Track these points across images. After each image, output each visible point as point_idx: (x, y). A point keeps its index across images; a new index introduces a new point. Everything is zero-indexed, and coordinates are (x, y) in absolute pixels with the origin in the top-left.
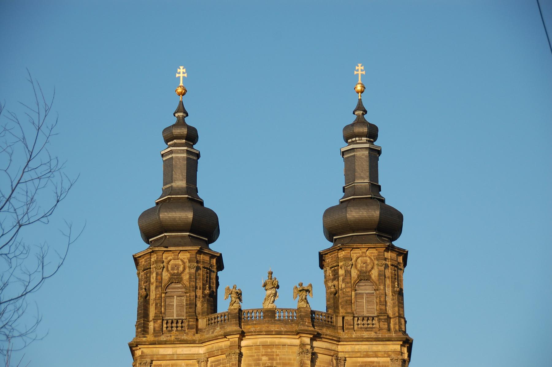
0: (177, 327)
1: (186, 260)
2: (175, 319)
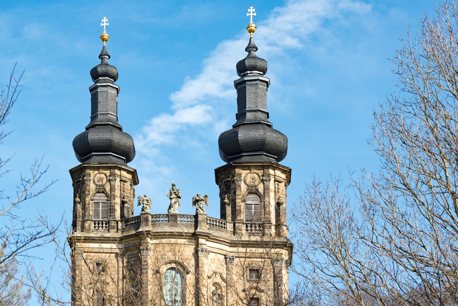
0: (102, 227)
1: (108, 174)
2: (101, 221)
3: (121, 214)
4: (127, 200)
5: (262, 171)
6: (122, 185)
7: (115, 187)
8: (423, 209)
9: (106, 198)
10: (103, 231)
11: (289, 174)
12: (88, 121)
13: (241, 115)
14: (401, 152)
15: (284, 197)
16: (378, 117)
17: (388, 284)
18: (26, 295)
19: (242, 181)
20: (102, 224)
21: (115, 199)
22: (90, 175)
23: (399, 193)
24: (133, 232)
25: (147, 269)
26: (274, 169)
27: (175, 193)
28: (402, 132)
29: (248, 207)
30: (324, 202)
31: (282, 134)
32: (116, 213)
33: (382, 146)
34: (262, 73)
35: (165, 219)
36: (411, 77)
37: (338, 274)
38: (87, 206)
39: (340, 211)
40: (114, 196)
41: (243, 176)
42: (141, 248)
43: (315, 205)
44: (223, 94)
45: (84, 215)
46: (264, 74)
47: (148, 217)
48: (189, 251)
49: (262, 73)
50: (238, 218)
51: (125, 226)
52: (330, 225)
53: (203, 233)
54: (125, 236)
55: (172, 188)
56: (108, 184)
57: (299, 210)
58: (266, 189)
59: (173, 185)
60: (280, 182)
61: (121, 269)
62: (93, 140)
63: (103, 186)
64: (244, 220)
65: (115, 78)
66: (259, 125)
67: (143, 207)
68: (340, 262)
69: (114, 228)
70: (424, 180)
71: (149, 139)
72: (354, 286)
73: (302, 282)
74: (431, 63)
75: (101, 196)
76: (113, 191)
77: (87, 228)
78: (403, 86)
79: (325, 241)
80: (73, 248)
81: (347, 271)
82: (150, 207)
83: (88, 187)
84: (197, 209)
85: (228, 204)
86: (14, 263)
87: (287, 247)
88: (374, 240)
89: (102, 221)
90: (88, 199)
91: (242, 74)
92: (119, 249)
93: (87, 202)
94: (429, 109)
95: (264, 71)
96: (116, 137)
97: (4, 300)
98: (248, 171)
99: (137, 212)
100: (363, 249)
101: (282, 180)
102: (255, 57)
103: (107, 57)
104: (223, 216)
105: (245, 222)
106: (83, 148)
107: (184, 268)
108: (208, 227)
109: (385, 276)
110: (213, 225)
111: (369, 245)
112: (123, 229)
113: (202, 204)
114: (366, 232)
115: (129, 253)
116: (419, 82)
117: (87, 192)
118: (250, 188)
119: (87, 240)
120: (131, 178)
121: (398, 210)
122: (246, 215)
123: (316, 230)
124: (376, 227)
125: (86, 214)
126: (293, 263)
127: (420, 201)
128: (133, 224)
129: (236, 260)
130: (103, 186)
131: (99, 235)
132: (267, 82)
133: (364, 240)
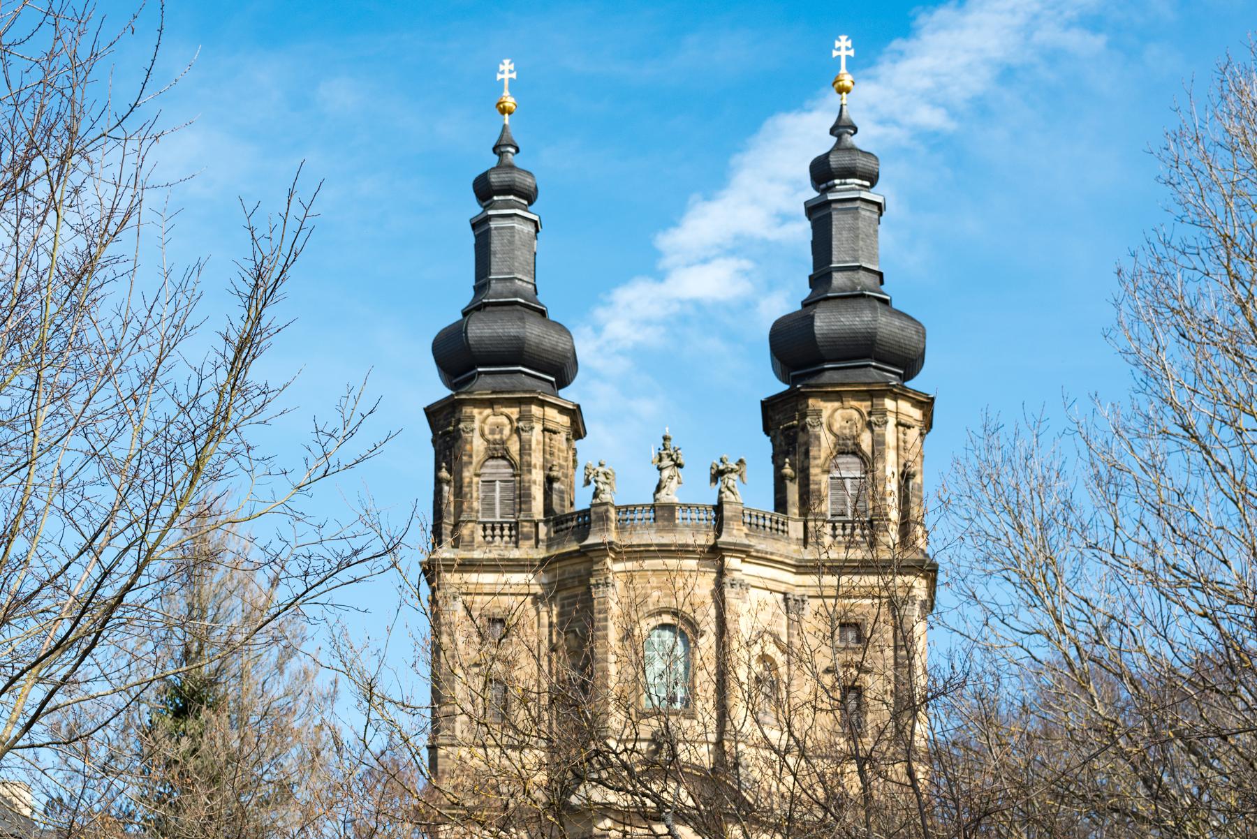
0: (502, 536)
4: (560, 474)
5: (869, 403)
8: (1224, 479)
9: (511, 470)
10: (503, 544)
12: (467, 296)
13: (821, 277)
14: (1175, 356)
16: (1128, 279)
17: (1146, 646)
18: (325, 693)
20: (502, 529)
21: (530, 472)
22: (472, 419)
23: (1171, 445)
24: (574, 546)
25: (605, 628)
26: (895, 397)
27: (670, 456)
28: (1178, 313)
30: (1009, 469)
33: (1137, 344)
34: (867, 184)
35: (647, 515)
36: (1198, 191)
37: (1038, 628)
38: (466, 489)
39: (1044, 487)
40: (529, 465)
42: (593, 581)
43: (990, 476)
44: (776, 234)
46: (873, 185)
47: (607, 511)
48: (705, 584)
49: (867, 184)
51: (556, 532)
52: (1021, 520)
53: (735, 544)
56: (515, 437)
58: (878, 443)
59: (665, 438)
60: (909, 427)
61: (546, 630)
62: (481, 340)
63: (503, 442)
65: (530, 196)
66: (862, 300)
68: (1043, 601)
69: (529, 538)
70: (1225, 415)
71: (609, 336)
72: (1073, 653)
73: (959, 648)
74: (1241, 160)
75: (498, 467)
77: (467, 538)
78: (1180, 211)
79: (1010, 556)
80: (434, 584)
81: (1059, 621)
83: (468, 447)
84: (721, 492)
85: (792, 479)
86: (298, 621)
88: (1119, 551)
89: (501, 523)
90: (467, 474)
91: (823, 186)
93: (466, 480)
94: (1236, 260)
95: (872, 178)
96: (533, 331)
97: (275, 705)
98: (837, 404)
99: (583, 500)
100: (1094, 570)
101: (914, 423)
102: (852, 149)
103: (513, 150)
104: (781, 504)
105: (829, 517)
106: (457, 357)
107: (692, 624)
109: (1141, 628)
111: (1106, 563)
113: (732, 480)
114: (1100, 535)
115: (564, 594)
116: (1214, 202)
117: (465, 458)
119: (468, 566)
121: (1169, 485)
122: (832, 503)
123: (991, 531)
124: (1123, 521)
125: (465, 506)
126: (939, 607)
127: (1217, 462)
130: (503, 442)
131: (494, 554)
132: (879, 205)
133: (1096, 551)
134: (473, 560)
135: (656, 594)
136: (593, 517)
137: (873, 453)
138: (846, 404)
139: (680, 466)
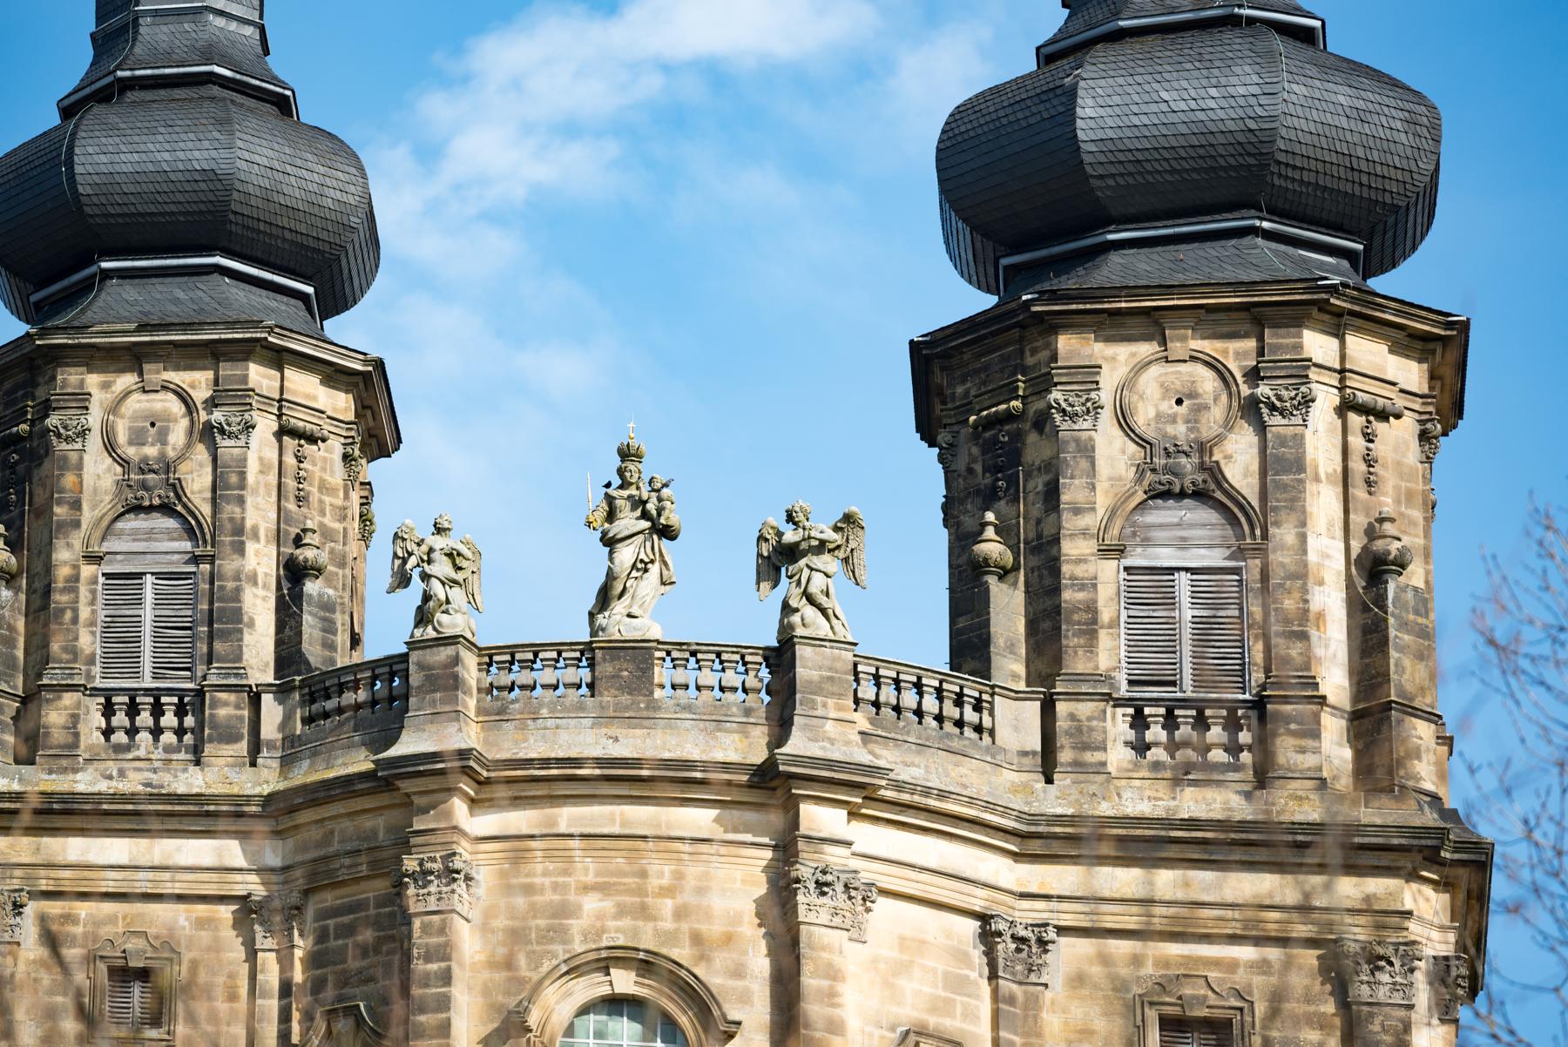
0: (157, 732)
1: (201, 394)
2: (147, 692)
3: (279, 643)
5: (1251, 344)
6: (290, 460)
7: (242, 475)
9: (187, 545)
10: (159, 754)
11: (1452, 355)
12: (72, 62)
15: (1417, 514)
19: (1107, 416)
20: (158, 710)
21: (240, 549)
22: (81, 400)
24: (359, 762)
25: (444, 1003)
26: (1337, 325)
29: (1151, 587)
31: (1395, 84)
32: (247, 638)
35: (571, 675)
38: (60, 598)
40: (239, 530)
41: (1109, 381)
45: (36, 656)
47: (456, 660)
48: (735, 882)
50: (1077, 663)
51: (308, 720)
53: (830, 764)
54: (304, 788)
55: (621, 472)
56: (201, 453)
57: (1531, 607)
58: (1282, 467)
59: (627, 454)
60: (1383, 416)
61: (272, 1005)
64: (1122, 679)
66: (1228, 35)
67: (427, 597)
69: (231, 737)
75: (150, 535)
76: (228, 499)
77: (58, 736)
82: (471, 599)
83: (69, 480)
84: (787, 609)
85: (1004, 574)
87: (1442, 863)
89: (156, 694)
90: (64, 555)
92: (258, 871)
93: (63, 572)
96: (254, 157)
98: (1146, 349)
99: (386, 628)
101: (1401, 402)
104: (970, 647)
105: (1123, 690)
108: (864, 725)
110: (897, 709)
112: (290, 740)
113: (823, 573)
115: (329, 899)
117: (60, 511)
118: (1160, 461)
120: (351, 417)
125: (55, 647)
126: (1493, 982)
128: (358, 706)
129: (1068, 954)
131: (132, 783)
134: (73, 797)
135: (592, 904)
136: (415, 679)
137: (1264, 495)
138: (1177, 348)
139: (667, 533)
